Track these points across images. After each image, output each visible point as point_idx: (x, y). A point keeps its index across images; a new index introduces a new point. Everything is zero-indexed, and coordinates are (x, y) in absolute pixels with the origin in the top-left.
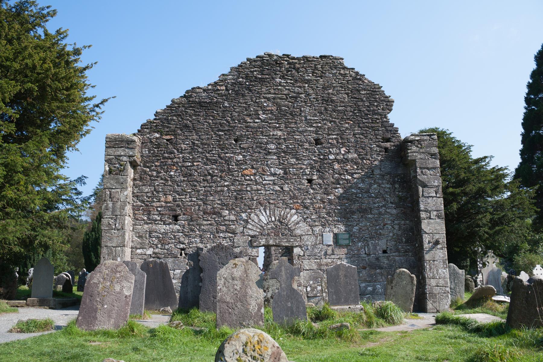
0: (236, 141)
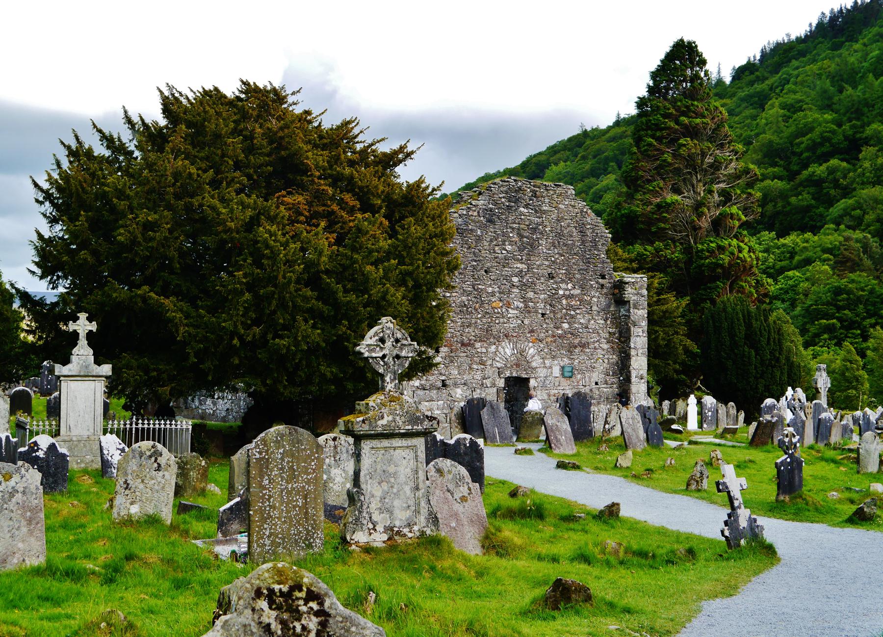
0: (486, 271)
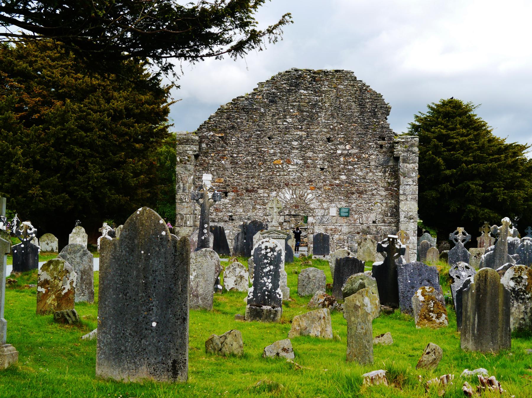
0: (269, 138)
